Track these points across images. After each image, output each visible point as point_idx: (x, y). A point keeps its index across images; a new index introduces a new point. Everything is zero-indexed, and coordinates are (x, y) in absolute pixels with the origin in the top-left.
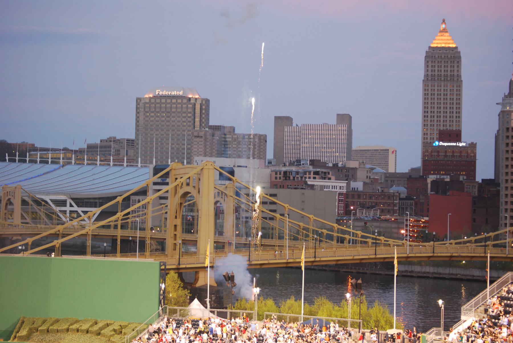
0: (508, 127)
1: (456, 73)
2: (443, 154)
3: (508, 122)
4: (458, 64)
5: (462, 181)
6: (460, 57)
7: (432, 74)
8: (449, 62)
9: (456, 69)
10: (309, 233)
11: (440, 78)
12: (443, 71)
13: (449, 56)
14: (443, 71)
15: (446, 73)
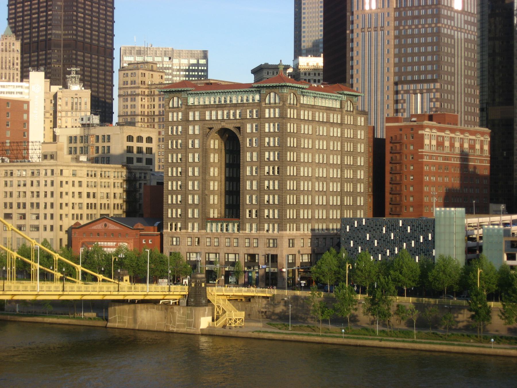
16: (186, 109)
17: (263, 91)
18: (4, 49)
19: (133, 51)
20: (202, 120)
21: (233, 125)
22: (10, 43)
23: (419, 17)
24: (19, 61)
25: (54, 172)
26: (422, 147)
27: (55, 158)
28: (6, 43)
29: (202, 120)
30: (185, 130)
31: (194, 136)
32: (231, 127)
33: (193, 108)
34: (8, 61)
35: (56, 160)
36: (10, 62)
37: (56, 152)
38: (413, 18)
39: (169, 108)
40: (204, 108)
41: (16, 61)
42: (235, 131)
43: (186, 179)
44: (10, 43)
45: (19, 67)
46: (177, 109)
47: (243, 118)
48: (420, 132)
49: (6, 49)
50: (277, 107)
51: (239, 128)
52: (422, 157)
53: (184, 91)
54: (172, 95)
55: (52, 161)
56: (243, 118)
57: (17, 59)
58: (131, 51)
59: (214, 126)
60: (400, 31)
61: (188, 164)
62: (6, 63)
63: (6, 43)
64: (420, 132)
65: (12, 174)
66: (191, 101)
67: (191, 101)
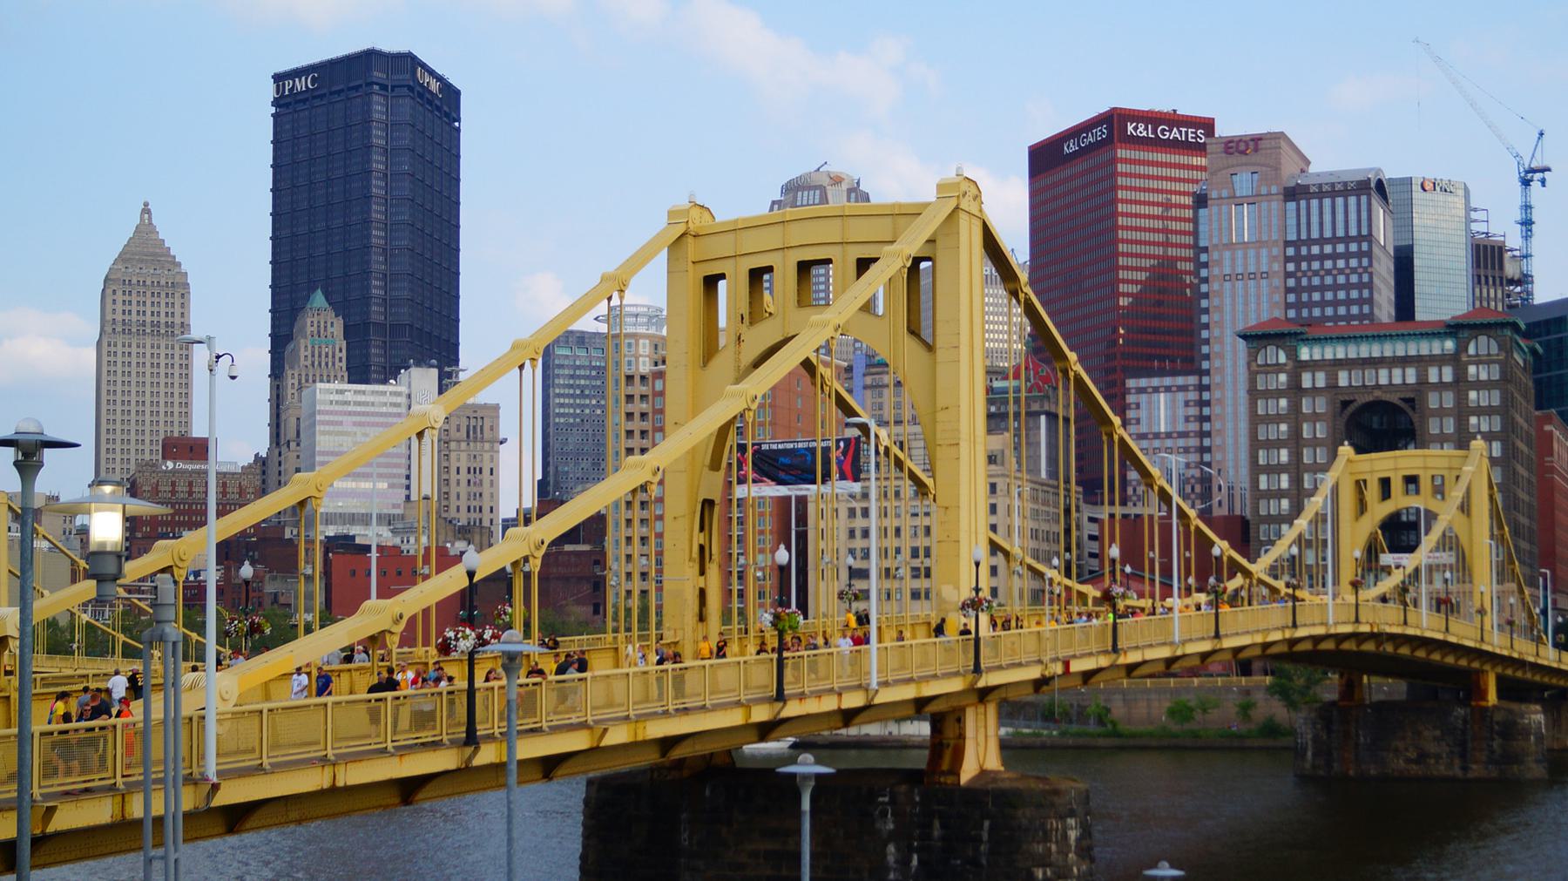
0: (630, 373)
1: (178, 320)
2: (185, 489)
3: (629, 363)
4: (182, 301)
5: (291, 539)
6: (186, 286)
7: (124, 320)
8: (163, 295)
9: (178, 310)
10: (124, 644)
11: (156, 329)
12: (149, 313)
13: (163, 282)
14: (149, 313)
15: (155, 319)
16: (1296, 367)
17: (1465, 334)
18: (316, 332)
19: (570, 339)
20: (1332, 386)
21: (1399, 395)
22: (326, 322)
23: (1334, 256)
24: (344, 354)
25: (998, 489)
26: (1552, 455)
27: (999, 461)
28: (319, 322)
29: (1332, 386)
30: (1295, 407)
31: (1315, 417)
32: (1394, 398)
33: (1313, 366)
34: (323, 353)
35: (1003, 464)
36: (327, 356)
37: (1003, 452)
38: (1322, 257)
39: (1259, 366)
40: (1334, 365)
41: (338, 355)
42: (1402, 404)
43: (1299, 495)
44: (326, 322)
45: (344, 364)
46: (1278, 368)
47: (1423, 382)
48: (1548, 428)
49: (319, 332)
50: (1494, 362)
51: (1410, 401)
52: (1552, 470)
53: (1296, 334)
54: (1264, 342)
55: (993, 467)
56: (1423, 382)
57: (341, 350)
58: (567, 337)
59: (1357, 397)
60: (1298, 280)
61: (1302, 467)
62: (320, 356)
63: (319, 322)
64: (1548, 428)
65: (897, 494)
66: (1305, 354)
67: (1305, 354)
